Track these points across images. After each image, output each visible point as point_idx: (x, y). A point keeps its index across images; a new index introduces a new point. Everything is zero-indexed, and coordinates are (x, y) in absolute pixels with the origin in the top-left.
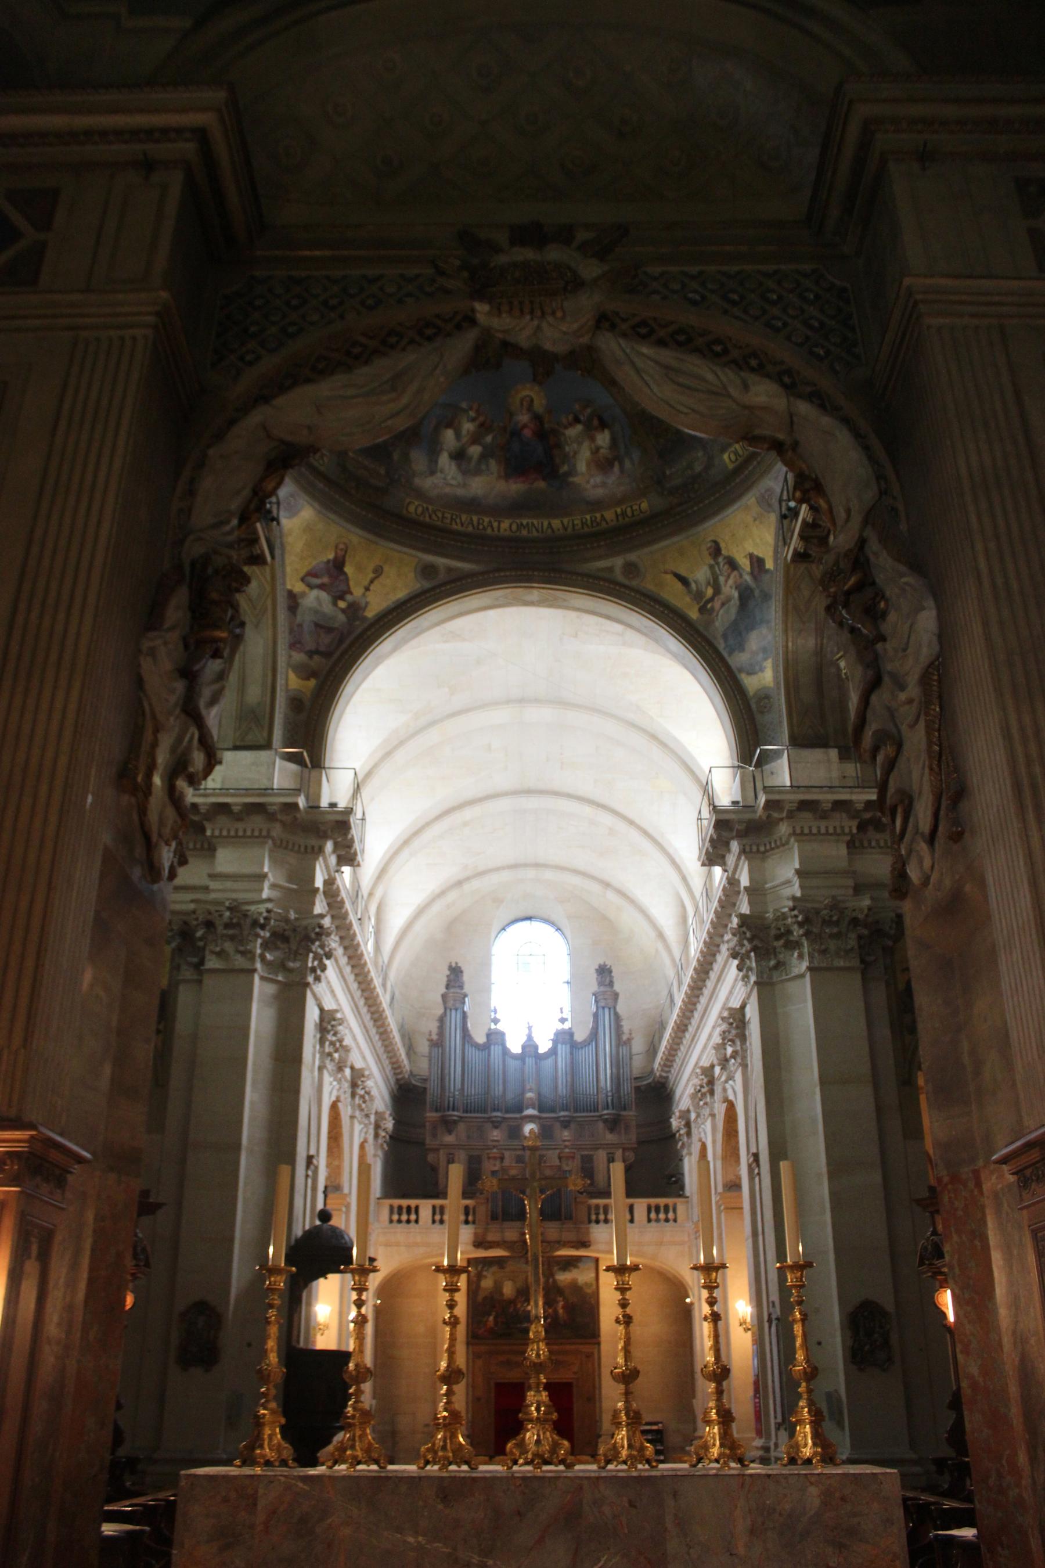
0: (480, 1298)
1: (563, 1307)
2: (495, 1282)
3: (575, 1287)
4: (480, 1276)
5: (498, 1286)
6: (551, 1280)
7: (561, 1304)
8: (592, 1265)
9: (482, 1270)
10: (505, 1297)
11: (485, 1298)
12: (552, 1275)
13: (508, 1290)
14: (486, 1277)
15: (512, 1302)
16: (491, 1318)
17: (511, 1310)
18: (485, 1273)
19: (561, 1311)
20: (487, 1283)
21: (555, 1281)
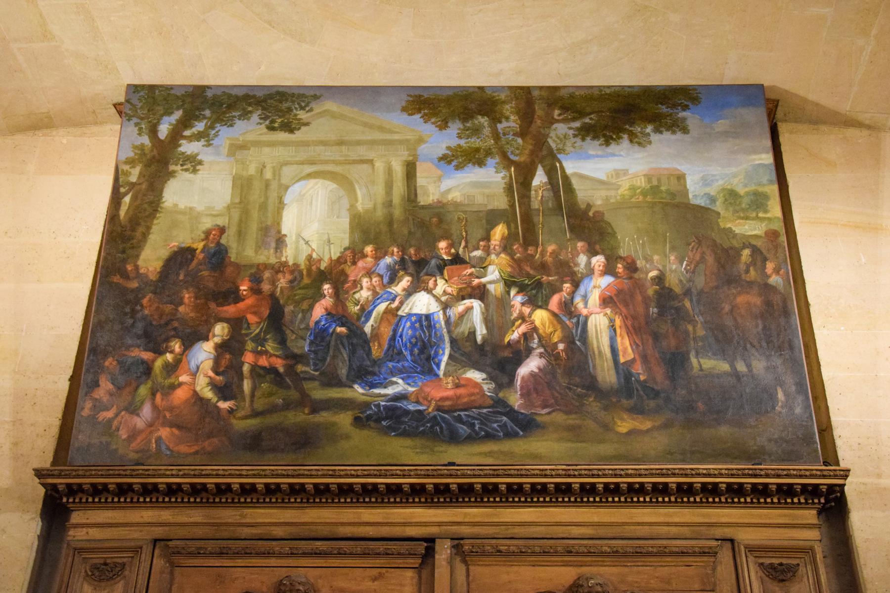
0: (151, 258)
1: (606, 301)
2: (242, 185)
3: (674, 211)
4: (159, 162)
5: (257, 203)
6: (540, 178)
7: (598, 285)
8: (757, 116)
9: (176, 135)
10: (293, 253)
11: (181, 257)
12: (550, 160)
13: (312, 222)
14: (193, 163)
15: (335, 275)
16: (203, 354)
17: (318, 312)
18: (187, 147)
19: (599, 322)
20: (199, 196)
21: (561, 185)
